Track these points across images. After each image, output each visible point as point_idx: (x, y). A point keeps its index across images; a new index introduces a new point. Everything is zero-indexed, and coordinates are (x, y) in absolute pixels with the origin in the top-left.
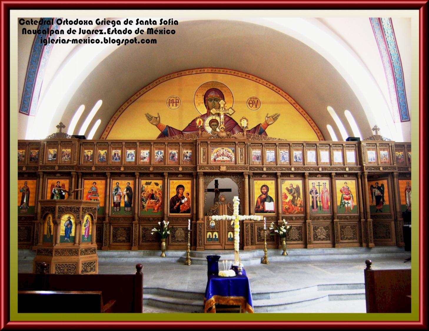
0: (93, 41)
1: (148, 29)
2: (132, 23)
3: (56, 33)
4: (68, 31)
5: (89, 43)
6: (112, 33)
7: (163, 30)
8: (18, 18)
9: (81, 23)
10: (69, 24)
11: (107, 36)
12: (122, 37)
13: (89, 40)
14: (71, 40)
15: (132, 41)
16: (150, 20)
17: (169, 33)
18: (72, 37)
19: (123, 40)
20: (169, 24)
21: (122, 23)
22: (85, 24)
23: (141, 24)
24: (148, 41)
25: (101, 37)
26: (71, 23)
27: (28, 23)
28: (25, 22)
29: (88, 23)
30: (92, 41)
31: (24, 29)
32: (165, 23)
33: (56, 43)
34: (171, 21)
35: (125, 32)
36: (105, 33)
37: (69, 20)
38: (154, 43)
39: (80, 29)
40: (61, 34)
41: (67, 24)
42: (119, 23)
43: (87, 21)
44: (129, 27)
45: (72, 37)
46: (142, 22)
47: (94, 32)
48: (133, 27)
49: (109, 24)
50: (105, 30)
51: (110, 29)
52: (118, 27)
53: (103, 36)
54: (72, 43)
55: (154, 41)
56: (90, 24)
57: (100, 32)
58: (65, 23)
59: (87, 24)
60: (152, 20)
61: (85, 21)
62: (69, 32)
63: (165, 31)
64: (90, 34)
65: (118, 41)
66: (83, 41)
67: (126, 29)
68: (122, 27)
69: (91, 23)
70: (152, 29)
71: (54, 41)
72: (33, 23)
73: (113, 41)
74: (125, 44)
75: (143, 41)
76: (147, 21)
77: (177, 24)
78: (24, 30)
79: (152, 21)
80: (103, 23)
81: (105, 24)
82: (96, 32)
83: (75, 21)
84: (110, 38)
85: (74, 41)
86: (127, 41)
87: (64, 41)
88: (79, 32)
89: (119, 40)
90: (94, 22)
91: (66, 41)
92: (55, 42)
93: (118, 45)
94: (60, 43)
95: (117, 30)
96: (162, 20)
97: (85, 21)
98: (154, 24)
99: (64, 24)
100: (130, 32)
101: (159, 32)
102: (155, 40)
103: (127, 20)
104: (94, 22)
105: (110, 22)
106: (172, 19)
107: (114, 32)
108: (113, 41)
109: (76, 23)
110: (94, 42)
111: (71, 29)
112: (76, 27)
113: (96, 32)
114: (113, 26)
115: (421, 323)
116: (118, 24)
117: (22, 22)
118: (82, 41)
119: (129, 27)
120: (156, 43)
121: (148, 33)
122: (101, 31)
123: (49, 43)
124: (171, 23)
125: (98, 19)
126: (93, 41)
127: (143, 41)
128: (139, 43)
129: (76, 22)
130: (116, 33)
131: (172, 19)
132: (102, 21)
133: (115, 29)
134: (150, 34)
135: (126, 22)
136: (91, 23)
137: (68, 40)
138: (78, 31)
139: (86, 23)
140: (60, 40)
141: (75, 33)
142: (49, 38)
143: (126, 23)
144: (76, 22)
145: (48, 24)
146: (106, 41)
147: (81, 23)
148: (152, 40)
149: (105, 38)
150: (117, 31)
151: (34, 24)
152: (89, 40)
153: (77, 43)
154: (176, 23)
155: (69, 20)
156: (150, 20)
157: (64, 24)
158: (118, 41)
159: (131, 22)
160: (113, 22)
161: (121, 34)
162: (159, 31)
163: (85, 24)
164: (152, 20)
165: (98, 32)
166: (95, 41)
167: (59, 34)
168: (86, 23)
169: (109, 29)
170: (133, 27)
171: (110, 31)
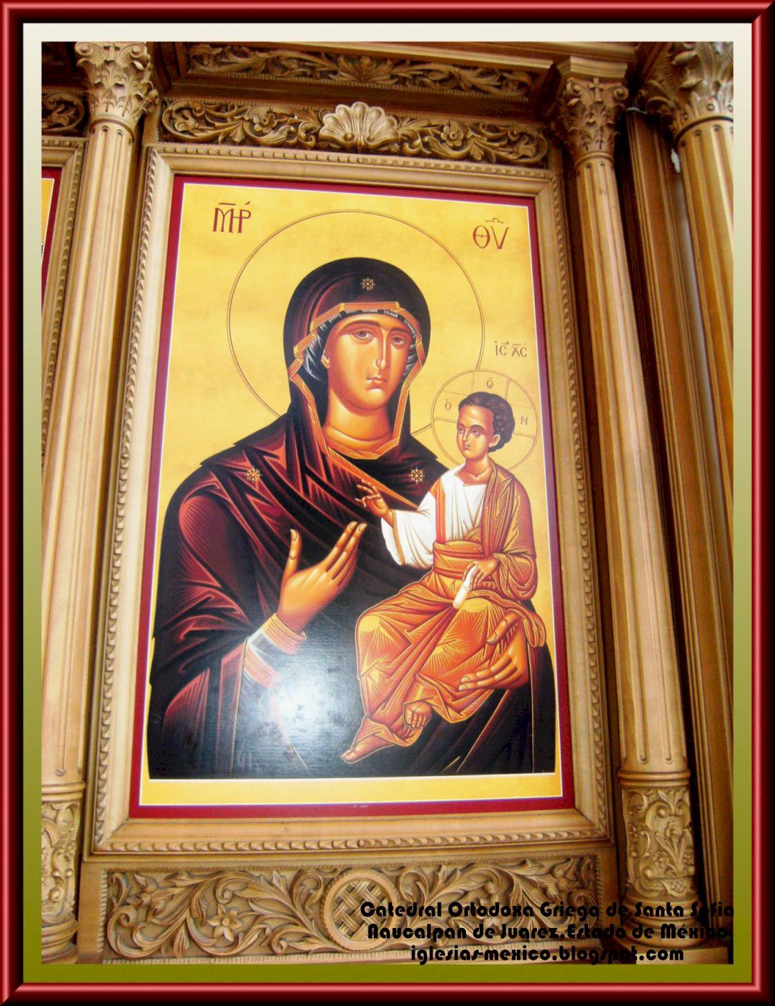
1: (665, 926)
14: (484, 951)
29: (522, 911)
33: (448, 958)
38: (677, 959)
54: (486, 959)
57: (549, 934)
58: (469, 912)
67: (612, 925)
71: (443, 954)
72: (394, 911)
85: (491, 955)
91: (472, 954)
99: (466, 914)
109: (494, 911)
120: (682, 958)
133: (586, 925)
134: (668, 937)
137: (476, 952)
140: (456, 952)
143: (611, 911)
157: (466, 914)
162: (688, 930)
165: (546, 932)
167: (453, 937)
169: (571, 928)
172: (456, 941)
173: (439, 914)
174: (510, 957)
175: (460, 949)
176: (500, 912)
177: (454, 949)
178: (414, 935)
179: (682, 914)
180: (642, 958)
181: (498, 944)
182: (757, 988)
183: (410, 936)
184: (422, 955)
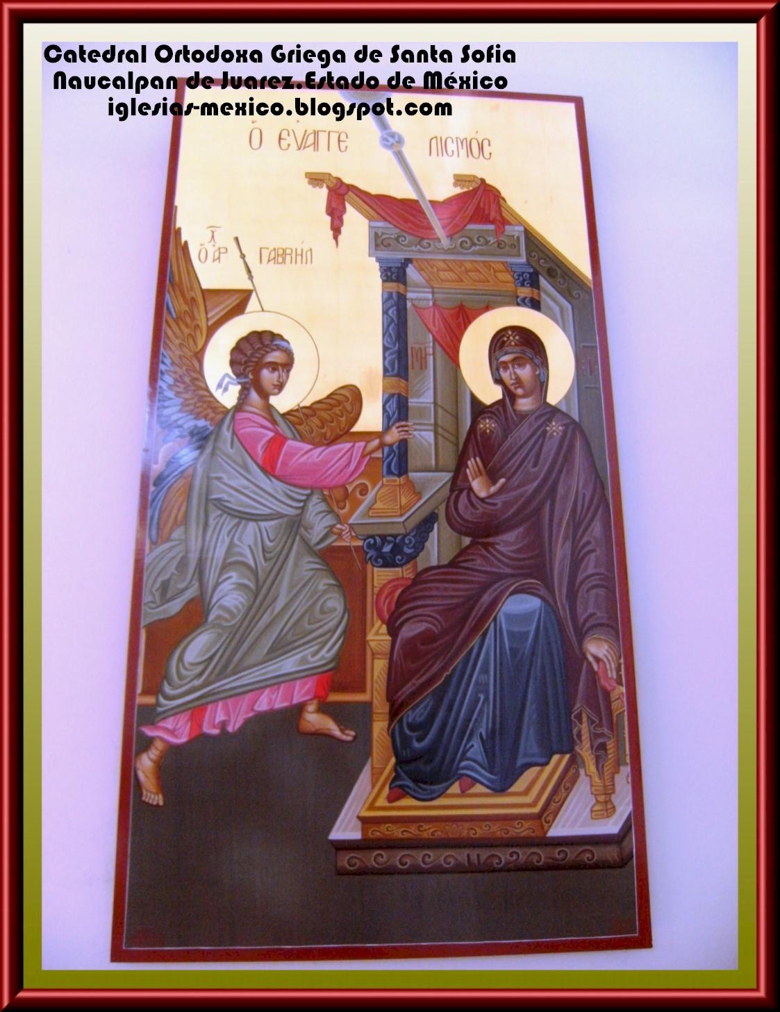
0: (263, 109)
1: (427, 74)
2: (379, 58)
3: (155, 87)
5: (251, 113)
7: (472, 76)
8: (43, 43)
9: (228, 56)
10: (191, 60)
13: (251, 105)
16: (433, 47)
17: (490, 85)
19: (352, 106)
20: (489, 61)
21: (350, 57)
22: (238, 61)
23: (405, 60)
25: (286, 97)
26: (198, 56)
27: (70, 56)
29: (248, 56)
30: (261, 109)
31: (60, 74)
32: (478, 56)
33: (155, 113)
34: (494, 51)
37: (191, 49)
38: (443, 113)
41: (187, 60)
42: (339, 56)
43: (245, 52)
44: (369, 68)
46: (408, 56)
49: (311, 61)
51: (313, 74)
54: (203, 113)
55: (445, 109)
56: (254, 60)
58: (181, 57)
59: (245, 61)
60: (439, 50)
61: (238, 52)
63: (475, 79)
65: (339, 109)
66: (235, 108)
67: (362, 74)
68: (349, 69)
69: (257, 56)
70: (438, 74)
71: (148, 107)
72: (86, 56)
73: (324, 109)
74: (359, 118)
75: (411, 109)
76: (422, 52)
77: (514, 60)
78: (60, 78)
79: (439, 53)
80: (294, 57)
81: (298, 60)
82: (273, 83)
83: (210, 52)
84: (313, 100)
86: (364, 109)
89: (341, 105)
90: (267, 56)
91: (185, 109)
92: (149, 112)
93: (338, 119)
95: (336, 76)
96: (466, 48)
97: (238, 52)
98: (444, 60)
99: (177, 60)
100: (373, 84)
101: (459, 82)
103: (365, 47)
104: (267, 56)
105: (313, 55)
106: (498, 46)
108: (324, 109)
112: (214, 70)
113: (273, 83)
114: (323, 66)
116: (337, 60)
117: (53, 54)
118: (231, 108)
119: (369, 68)
120: (450, 113)
123: (133, 113)
124: (494, 59)
125: (280, 47)
126: (263, 109)
127: (411, 109)
128: (399, 113)
131: (498, 46)
132: (291, 53)
133: (329, 73)
135: (362, 55)
136: (257, 56)
139: (242, 56)
140: (165, 105)
142: (133, 100)
143: (361, 56)
144: (213, 55)
145: (130, 60)
146: (302, 109)
147: (228, 56)
148: (438, 105)
149: (298, 100)
151: (87, 60)
152: (251, 105)
153: (216, 113)
154: (510, 56)
155: (191, 49)
156: (433, 47)
157: (177, 60)
158: (339, 109)
159: (376, 56)
160: (324, 56)
163: (238, 61)
164: (439, 50)
167: (161, 87)
168: (242, 56)
170: (383, 70)
173: (144, 60)
174: (233, 112)
175: (170, 103)
178: (112, 85)
179: (450, 60)
180: (399, 113)
181: (217, 95)
182: (762, 994)
183: (107, 86)
184: (122, 109)
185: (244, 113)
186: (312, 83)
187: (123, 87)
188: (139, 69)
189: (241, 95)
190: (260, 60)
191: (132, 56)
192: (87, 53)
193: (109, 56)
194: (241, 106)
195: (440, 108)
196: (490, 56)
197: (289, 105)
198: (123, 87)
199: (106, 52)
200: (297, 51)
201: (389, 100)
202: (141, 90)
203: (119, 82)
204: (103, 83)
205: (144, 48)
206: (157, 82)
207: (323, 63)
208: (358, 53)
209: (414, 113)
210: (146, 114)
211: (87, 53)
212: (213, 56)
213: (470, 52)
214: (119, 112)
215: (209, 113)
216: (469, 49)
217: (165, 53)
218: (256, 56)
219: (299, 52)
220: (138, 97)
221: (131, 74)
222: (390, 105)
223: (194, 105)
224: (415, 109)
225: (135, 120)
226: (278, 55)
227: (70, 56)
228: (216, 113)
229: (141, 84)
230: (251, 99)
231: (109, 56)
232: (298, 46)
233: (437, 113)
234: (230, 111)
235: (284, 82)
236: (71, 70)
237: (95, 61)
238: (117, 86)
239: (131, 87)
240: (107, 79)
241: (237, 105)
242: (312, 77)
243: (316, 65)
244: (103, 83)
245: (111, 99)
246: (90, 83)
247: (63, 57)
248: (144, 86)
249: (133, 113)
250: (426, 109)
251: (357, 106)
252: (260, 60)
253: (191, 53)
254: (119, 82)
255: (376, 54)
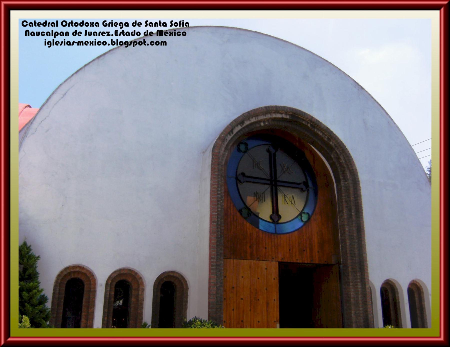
0: (99, 43)
1: (158, 31)
3: (61, 35)
4: (73, 33)
5: (95, 45)
6: (120, 35)
9: (87, 24)
10: (74, 26)
11: (115, 38)
12: (130, 39)
13: (95, 42)
15: (140, 43)
16: (160, 21)
18: (77, 39)
21: (130, 24)
22: (91, 26)
23: (150, 26)
24: (157, 43)
25: (108, 39)
26: (76, 24)
27: (31, 24)
28: (28, 23)
29: (94, 24)
30: (99, 43)
31: (27, 31)
33: (61, 45)
34: (181, 23)
35: (133, 34)
36: (112, 35)
37: (74, 22)
38: (164, 45)
39: (86, 31)
40: (66, 35)
41: (72, 26)
42: (126, 24)
43: (93, 23)
44: (137, 29)
45: (77, 39)
46: (151, 24)
47: (101, 34)
48: (142, 29)
49: (116, 26)
50: (112, 31)
51: (117, 31)
52: (126, 29)
53: (110, 38)
54: (78, 45)
55: (164, 43)
56: (96, 26)
57: (107, 34)
58: (70, 25)
59: (93, 26)
60: (162, 22)
61: (91, 23)
62: (75, 34)
64: (97, 35)
66: (89, 43)
67: (135, 31)
68: (130, 29)
69: (97, 24)
70: (162, 31)
71: (59, 43)
73: (121, 43)
74: (134, 46)
75: (152, 43)
76: (156, 23)
78: (27, 32)
79: (162, 23)
80: (111, 25)
81: (112, 26)
82: (103, 34)
83: (81, 23)
84: (117, 40)
85: (80, 43)
86: (135, 43)
87: (69, 43)
88: (85, 34)
90: (101, 24)
91: (72, 43)
92: (59, 44)
93: (126, 47)
94: (64, 45)
95: (125, 32)
96: (172, 22)
97: (91, 23)
98: (164, 26)
99: (69, 26)
100: (139, 34)
102: (165, 42)
103: (136, 21)
104: (101, 24)
105: (117, 24)
106: (183, 21)
107: (122, 34)
110: (100, 44)
111: (76, 31)
112: (82, 29)
113: (103, 34)
114: (121, 28)
115: (442, 339)
116: (126, 26)
117: (25, 24)
118: (88, 43)
119: (137, 29)
120: (166, 45)
121: (157, 35)
122: (108, 33)
123: (53, 45)
124: (181, 26)
125: (106, 21)
126: (99, 43)
127: (152, 43)
128: (148, 45)
129: (82, 24)
130: (124, 35)
131: (183, 21)
132: (110, 23)
133: (123, 31)
134: (160, 35)
135: (134, 24)
136: (97, 24)
137: (74, 42)
138: (84, 33)
139: (92, 24)
140: (65, 42)
141: (81, 35)
142: (53, 40)
143: (134, 24)
144: (82, 24)
145: (52, 26)
146: (113, 43)
148: (162, 42)
149: (112, 40)
150: (125, 33)
151: (37, 26)
152: (95, 42)
153: (83, 45)
155: (74, 22)
156: (160, 21)
157: (69, 26)
159: (140, 24)
160: (121, 24)
161: (129, 35)
163: (91, 26)
164: (162, 22)
165: (105, 33)
166: (102, 43)
167: (63, 35)
168: (92, 24)
169: (116, 31)
170: (142, 29)
171: (117, 33)
172: (64, 37)
173: (57, 26)
174: (89, 44)
176: (84, 25)
177: (64, 41)
179: (166, 26)
180: (148, 45)
181: (83, 38)
183: (44, 35)
184: (49, 43)
185: (93, 45)
186: (117, 34)
187: (50, 35)
188: (55, 29)
189: (92, 38)
190: (98, 26)
191: (53, 24)
192: (37, 23)
193: (45, 24)
194: (92, 42)
195: (162, 43)
196: (180, 24)
197: (109, 42)
198: (50, 35)
199: (44, 23)
200: (112, 23)
201: (144, 40)
202: (56, 37)
203: (48, 34)
204: (43, 34)
205: (57, 21)
206: (62, 34)
207: (121, 27)
208: (133, 23)
209: (153, 45)
210: (58, 45)
211: (37, 23)
212: (82, 24)
213: (173, 23)
214: (48, 44)
215: (80, 45)
216: (173, 22)
217: (64, 23)
218: (97, 24)
219: (112, 23)
220: (54, 39)
221: (52, 31)
222: (145, 42)
223: (75, 42)
224: (153, 43)
225: (54, 47)
226: (105, 24)
227: (31, 24)
228: (83, 45)
229: (56, 34)
230: (95, 40)
231: (45, 24)
232: (112, 21)
233: (161, 45)
234: (88, 44)
235: (107, 34)
236: (31, 29)
237: (40, 26)
238: (47, 35)
239: (52, 35)
240: (44, 32)
241: (90, 42)
242: (117, 32)
243: (118, 28)
244: (43, 34)
245: (45, 40)
246: (38, 34)
247: (28, 25)
248: (57, 35)
249: (53, 45)
250: (157, 43)
251: (133, 42)
252: (98, 26)
253: (74, 23)
254: (48, 34)
255: (140, 24)
